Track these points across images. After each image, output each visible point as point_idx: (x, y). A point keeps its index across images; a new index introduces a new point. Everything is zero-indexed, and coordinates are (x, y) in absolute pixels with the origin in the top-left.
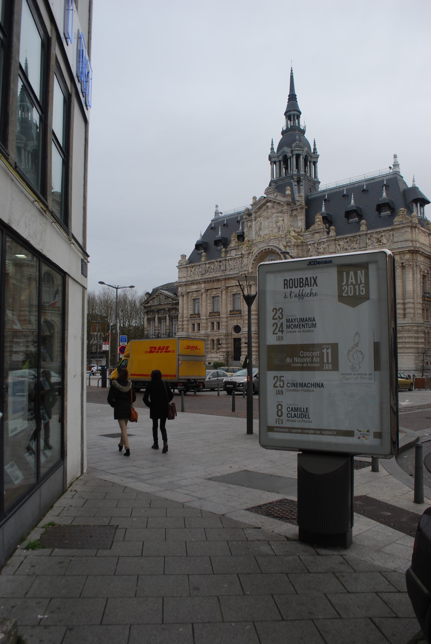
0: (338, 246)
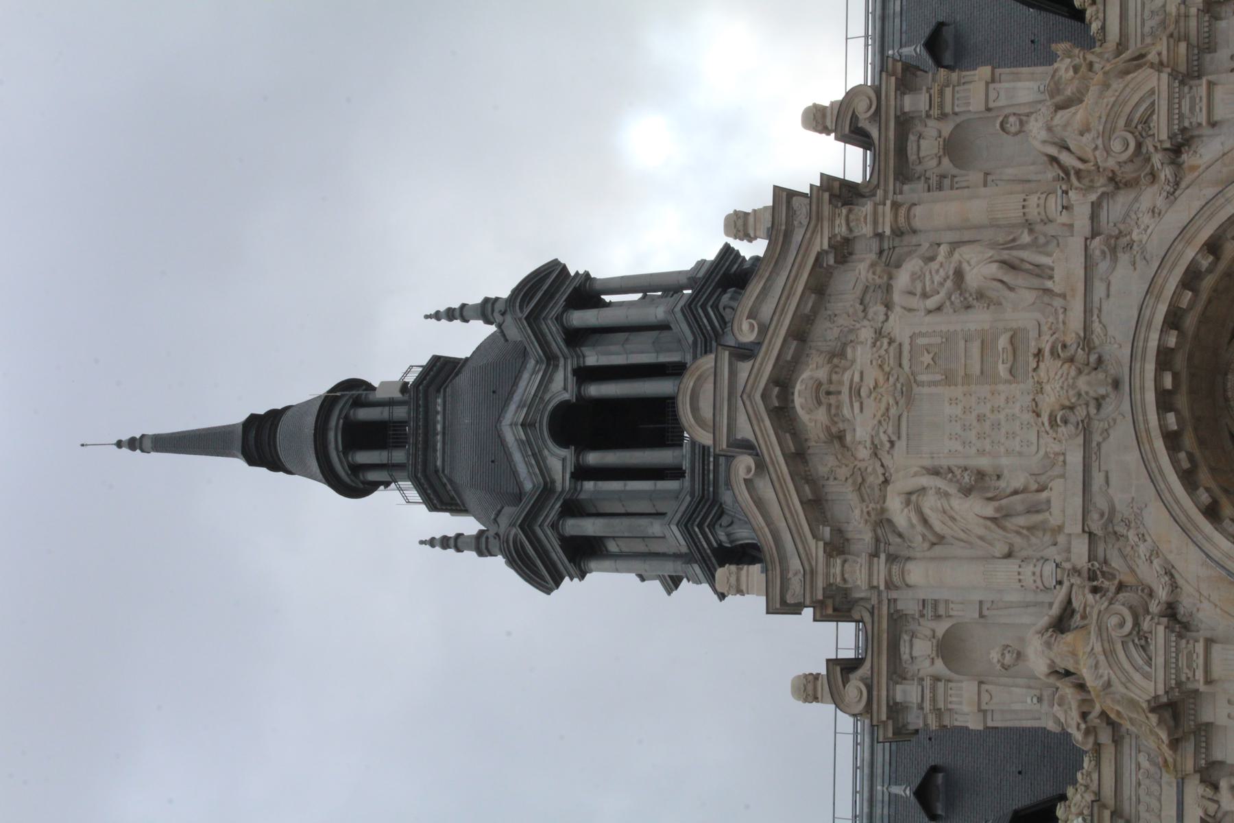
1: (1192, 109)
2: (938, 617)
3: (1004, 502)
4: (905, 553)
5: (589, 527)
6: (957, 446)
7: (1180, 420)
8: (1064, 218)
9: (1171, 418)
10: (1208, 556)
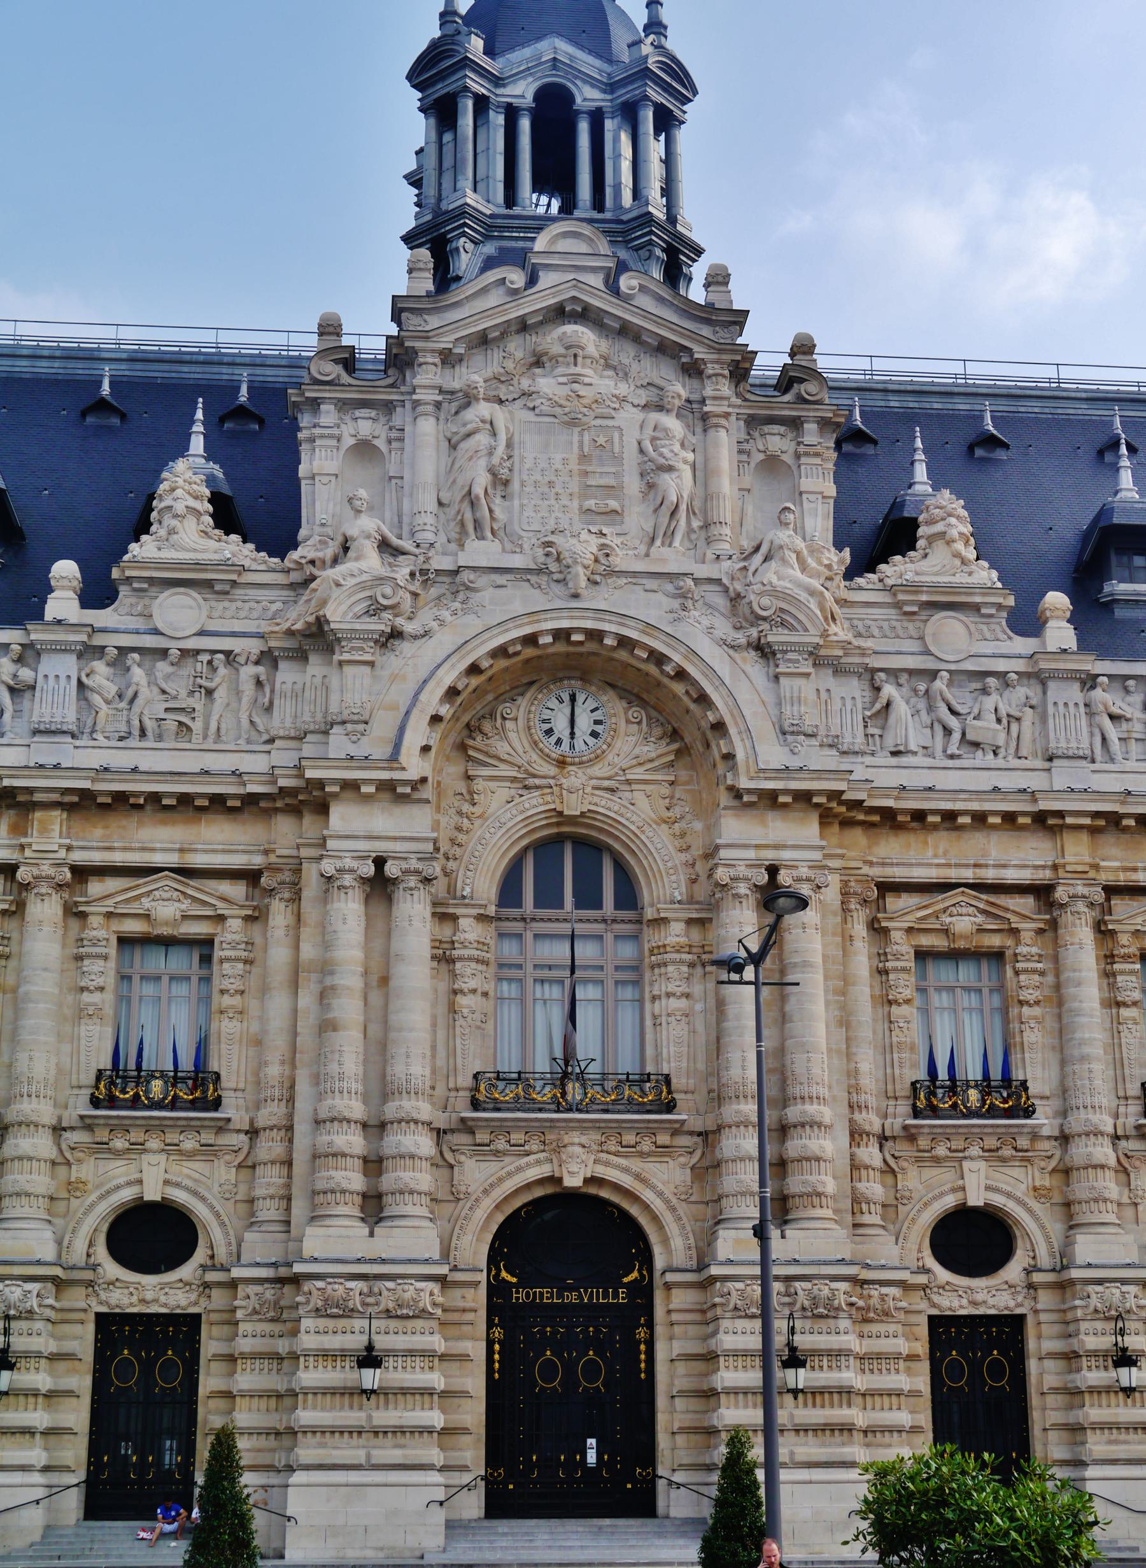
0: (1107, 722)
1: (790, 661)
2: (390, 442)
3: (483, 501)
4: (442, 416)
5: (466, 120)
6: (529, 464)
7: (546, 645)
8: (710, 556)
9: (549, 639)
10: (439, 666)
